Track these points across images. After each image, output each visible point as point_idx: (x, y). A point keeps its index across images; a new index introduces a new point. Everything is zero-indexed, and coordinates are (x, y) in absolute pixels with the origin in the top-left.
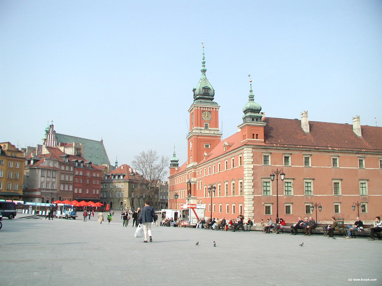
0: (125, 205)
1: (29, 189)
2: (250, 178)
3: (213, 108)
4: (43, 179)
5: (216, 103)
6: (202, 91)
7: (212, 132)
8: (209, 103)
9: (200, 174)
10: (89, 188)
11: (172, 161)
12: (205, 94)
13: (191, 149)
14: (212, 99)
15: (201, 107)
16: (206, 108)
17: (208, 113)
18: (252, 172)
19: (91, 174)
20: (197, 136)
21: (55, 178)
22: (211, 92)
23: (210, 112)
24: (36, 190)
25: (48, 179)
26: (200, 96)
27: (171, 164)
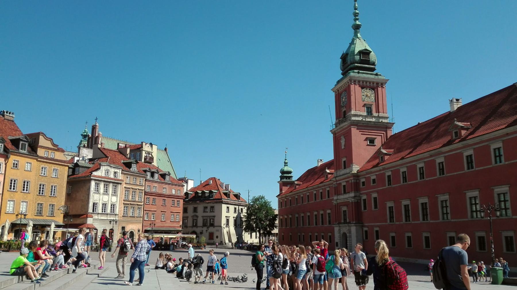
0: (217, 237)
9: (372, 184)
11: (283, 172)
12: (361, 62)
13: (343, 147)
14: (373, 70)
25: (105, 198)
26: (356, 64)
27: (282, 178)
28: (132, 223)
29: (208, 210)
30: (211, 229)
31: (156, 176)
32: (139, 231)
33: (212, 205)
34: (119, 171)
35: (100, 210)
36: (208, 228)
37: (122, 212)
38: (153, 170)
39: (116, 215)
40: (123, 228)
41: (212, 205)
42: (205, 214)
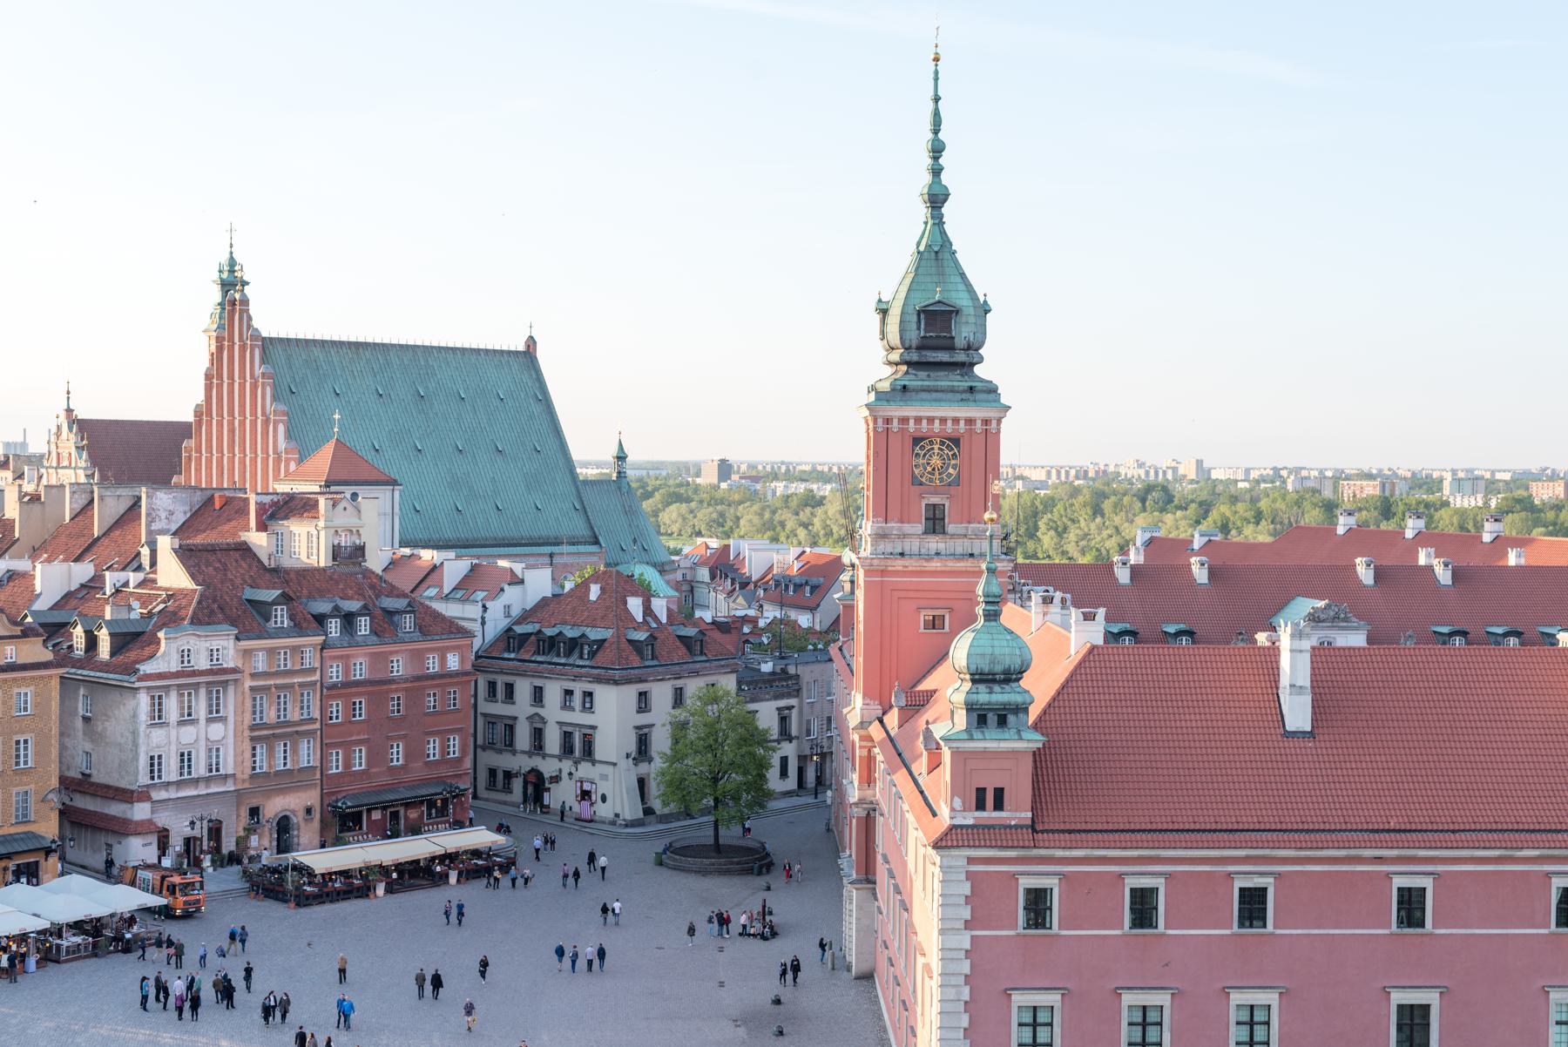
0: (604, 798)
1: (95, 779)
2: (951, 994)
3: (970, 421)
4: (158, 735)
5: (992, 390)
6: (914, 326)
7: (960, 546)
8: (952, 390)
10: (399, 738)
15: (904, 420)
16: (931, 420)
17: (942, 443)
18: (966, 967)
19: (419, 656)
20: (883, 573)
21: (223, 720)
22: (962, 332)
23: (956, 441)
24: (127, 796)
28: (283, 791)
29: (577, 699)
30: (585, 770)
31: (364, 626)
32: (309, 811)
33: (589, 687)
34: (230, 643)
35: (171, 772)
36: (576, 763)
37: (248, 764)
38: (353, 605)
39: (226, 776)
40: (254, 812)
41: (589, 687)
42: (568, 717)
